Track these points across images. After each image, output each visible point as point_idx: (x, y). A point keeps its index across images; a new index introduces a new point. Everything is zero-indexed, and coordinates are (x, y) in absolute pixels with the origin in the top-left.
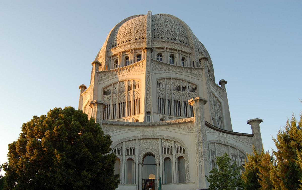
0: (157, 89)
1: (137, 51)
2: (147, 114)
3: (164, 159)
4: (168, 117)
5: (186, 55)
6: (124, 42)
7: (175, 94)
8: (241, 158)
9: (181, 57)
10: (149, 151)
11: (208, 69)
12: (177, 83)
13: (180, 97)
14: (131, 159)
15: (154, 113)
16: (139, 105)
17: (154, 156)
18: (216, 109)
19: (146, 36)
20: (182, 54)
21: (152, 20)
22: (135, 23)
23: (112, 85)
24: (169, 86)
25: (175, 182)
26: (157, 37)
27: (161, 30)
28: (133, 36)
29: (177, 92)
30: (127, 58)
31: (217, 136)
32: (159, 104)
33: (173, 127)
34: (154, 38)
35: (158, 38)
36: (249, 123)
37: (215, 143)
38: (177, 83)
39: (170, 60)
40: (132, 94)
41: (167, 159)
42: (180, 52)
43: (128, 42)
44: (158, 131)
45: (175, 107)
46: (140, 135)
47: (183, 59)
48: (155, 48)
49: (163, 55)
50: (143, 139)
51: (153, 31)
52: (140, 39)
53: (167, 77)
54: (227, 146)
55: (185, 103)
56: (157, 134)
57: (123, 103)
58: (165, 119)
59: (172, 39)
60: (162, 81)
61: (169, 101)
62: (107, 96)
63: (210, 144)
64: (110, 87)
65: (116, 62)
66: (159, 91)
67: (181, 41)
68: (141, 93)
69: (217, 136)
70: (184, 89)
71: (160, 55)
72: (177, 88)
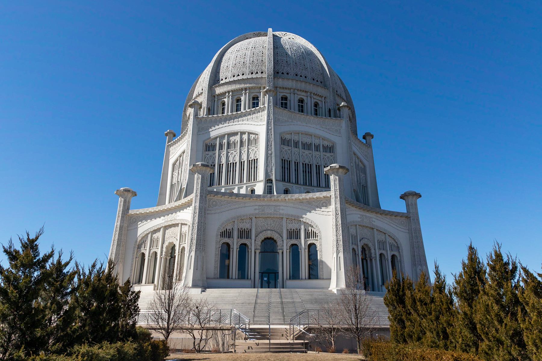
0: (280, 148)
1: (252, 91)
2: (267, 183)
5: (320, 99)
6: (234, 76)
8: (391, 246)
9: (313, 101)
10: (269, 234)
11: (350, 117)
12: (307, 140)
14: (245, 244)
15: (276, 180)
16: (256, 168)
17: (275, 241)
18: (358, 175)
19: (265, 69)
20: (315, 97)
21: (274, 47)
22: (250, 49)
24: (296, 144)
25: (304, 277)
26: (281, 72)
28: (248, 68)
29: (307, 152)
30: (239, 100)
31: (359, 216)
32: (283, 168)
34: (278, 73)
35: (283, 73)
36: (401, 197)
39: (299, 105)
40: (246, 152)
42: (312, 94)
43: (240, 77)
44: (281, 208)
45: (304, 172)
46: (257, 211)
47: (316, 105)
48: (278, 89)
51: (276, 62)
52: (257, 73)
54: (373, 229)
55: (318, 168)
56: (281, 212)
59: (301, 76)
60: (288, 137)
61: (297, 164)
65: (224, 104)
66: (283, 150)
67: (314, 80)
68: (259, 152)
69: (359, 216)
70: (317, 148)
71: (285, 98)
72: (307, 146)
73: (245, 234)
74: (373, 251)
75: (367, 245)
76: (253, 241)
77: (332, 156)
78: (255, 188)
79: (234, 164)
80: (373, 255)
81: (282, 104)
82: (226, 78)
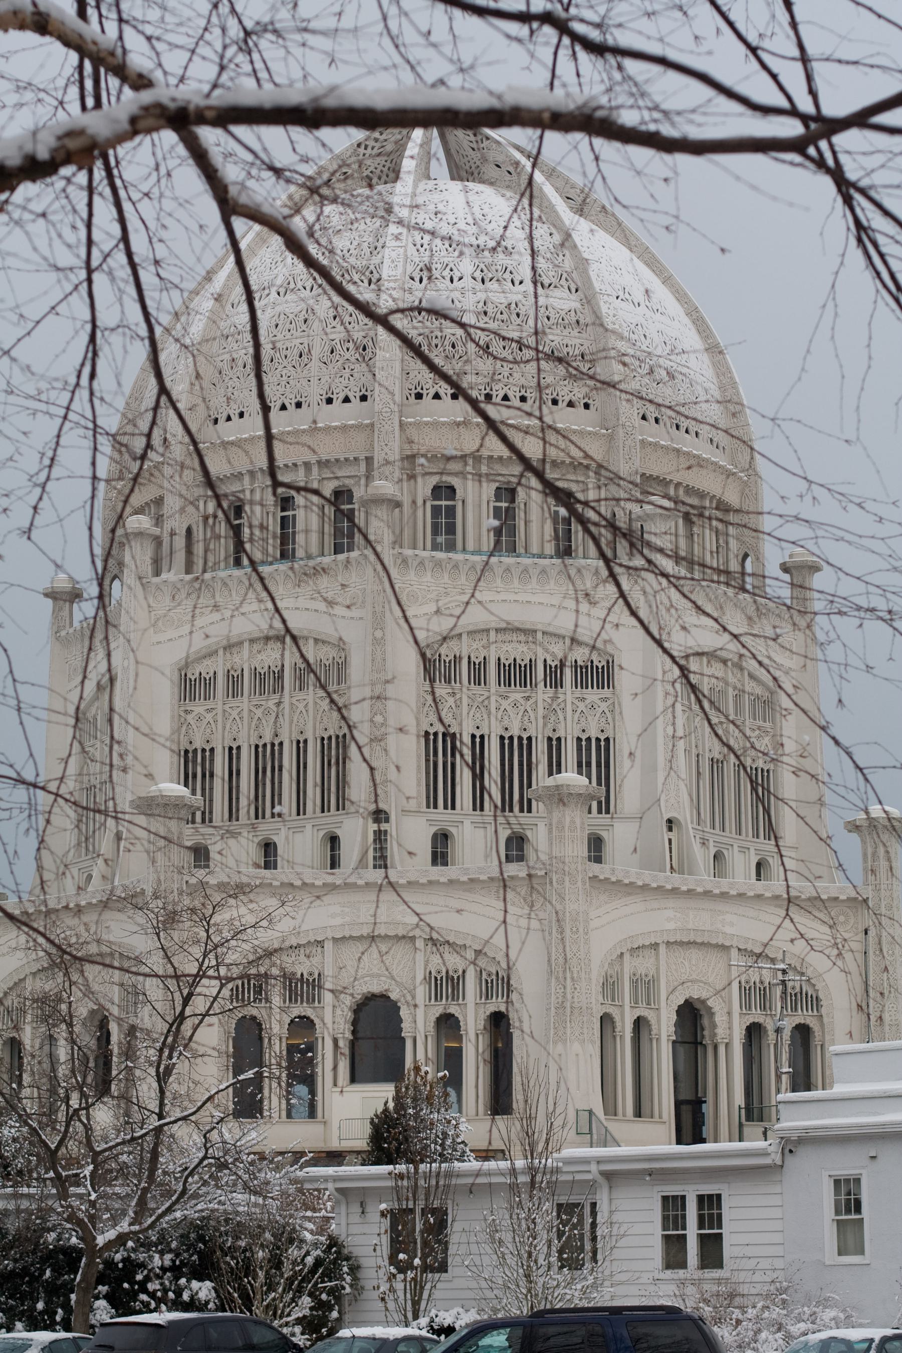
3: (433, 1019)
4: (467, 823)
7: (505, 704)
10: (376, 989)
12: (515, 651)
13: (533, 719)
23: (221, 652)
25: (472, 1111)
27: (453, 346)
28: (315, 381)
29: (517, 694)
33: (469, 890)
37: (657, 944)
38: (523, 648)
41: (448, 1024)
49: (459, 493)
50: (351, 937)
53: (471, 628)
54: (724, 948)
57: (273, 745)
58: (453, 830)
61: (479, 743)
62: (199, 708)
63: (627, 957)
64: (207, 662)
72: (516, 675)
73: (304, 988)
74: (720, 1019)
75: (703, 1002)
76: (328, 1011)
77: (605, 700)
78: (339, 832)
79: (276, 748)
80: (721, 1032)
81: (436, 510)
82: (241, 415)
